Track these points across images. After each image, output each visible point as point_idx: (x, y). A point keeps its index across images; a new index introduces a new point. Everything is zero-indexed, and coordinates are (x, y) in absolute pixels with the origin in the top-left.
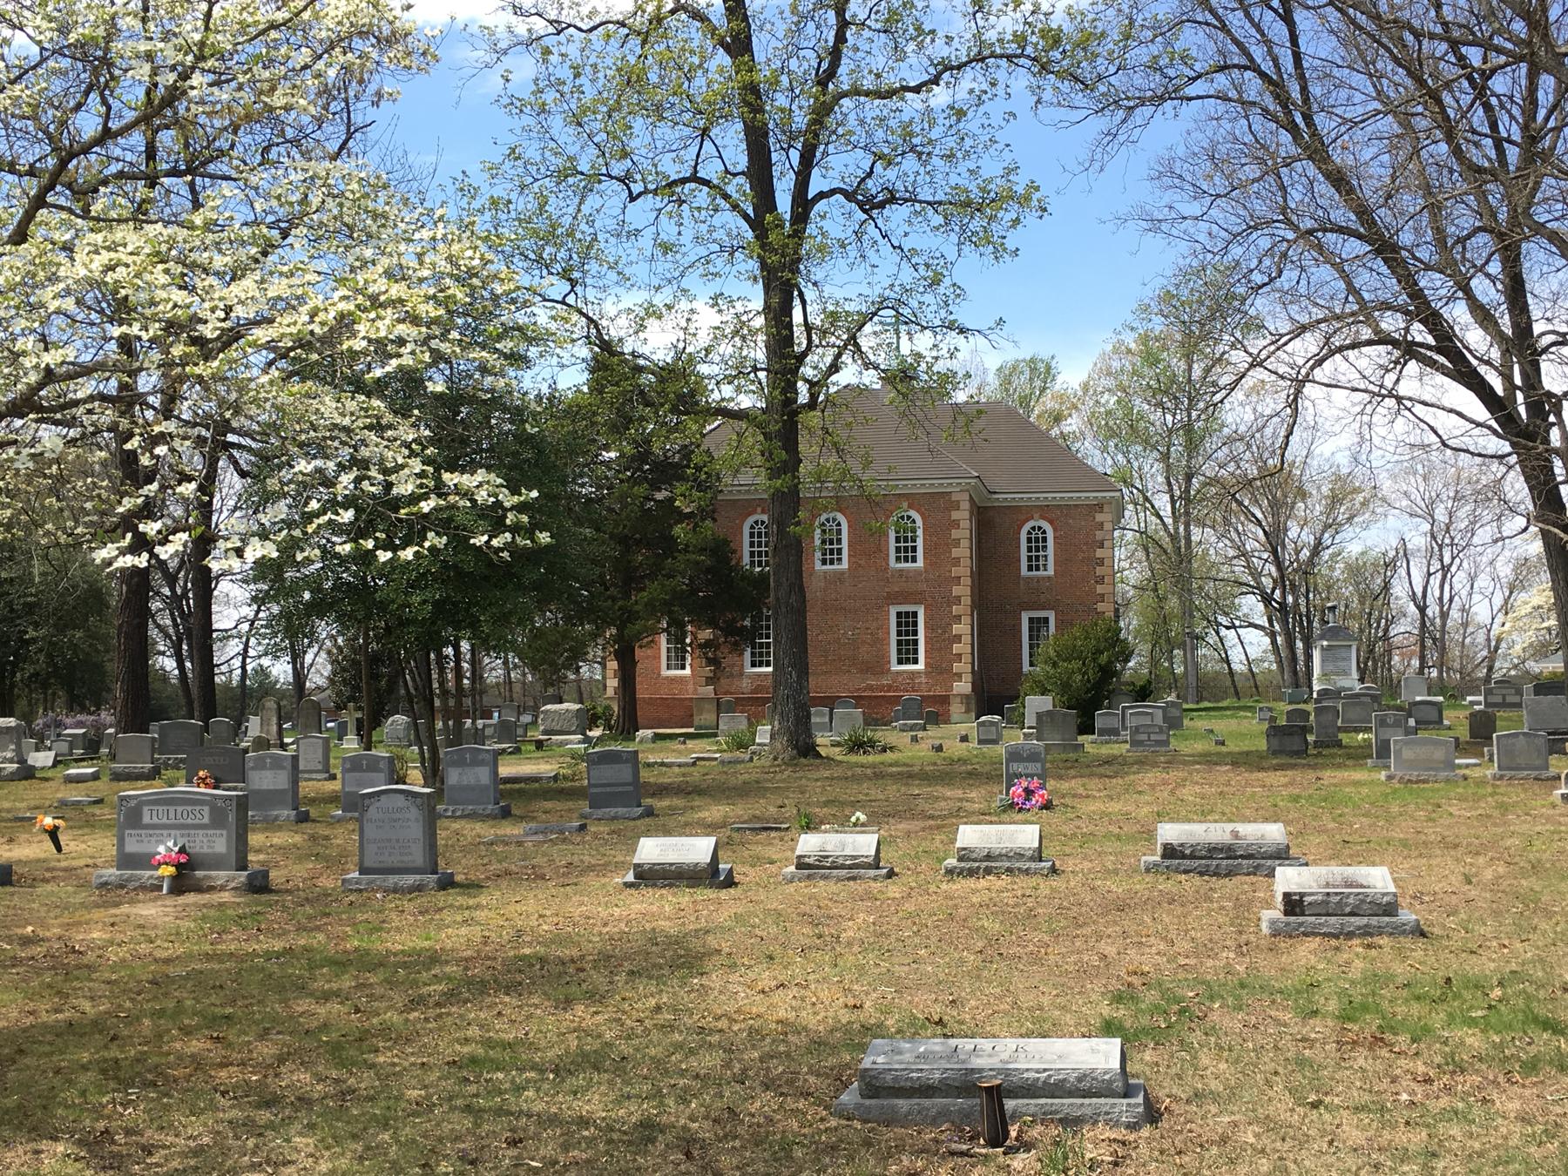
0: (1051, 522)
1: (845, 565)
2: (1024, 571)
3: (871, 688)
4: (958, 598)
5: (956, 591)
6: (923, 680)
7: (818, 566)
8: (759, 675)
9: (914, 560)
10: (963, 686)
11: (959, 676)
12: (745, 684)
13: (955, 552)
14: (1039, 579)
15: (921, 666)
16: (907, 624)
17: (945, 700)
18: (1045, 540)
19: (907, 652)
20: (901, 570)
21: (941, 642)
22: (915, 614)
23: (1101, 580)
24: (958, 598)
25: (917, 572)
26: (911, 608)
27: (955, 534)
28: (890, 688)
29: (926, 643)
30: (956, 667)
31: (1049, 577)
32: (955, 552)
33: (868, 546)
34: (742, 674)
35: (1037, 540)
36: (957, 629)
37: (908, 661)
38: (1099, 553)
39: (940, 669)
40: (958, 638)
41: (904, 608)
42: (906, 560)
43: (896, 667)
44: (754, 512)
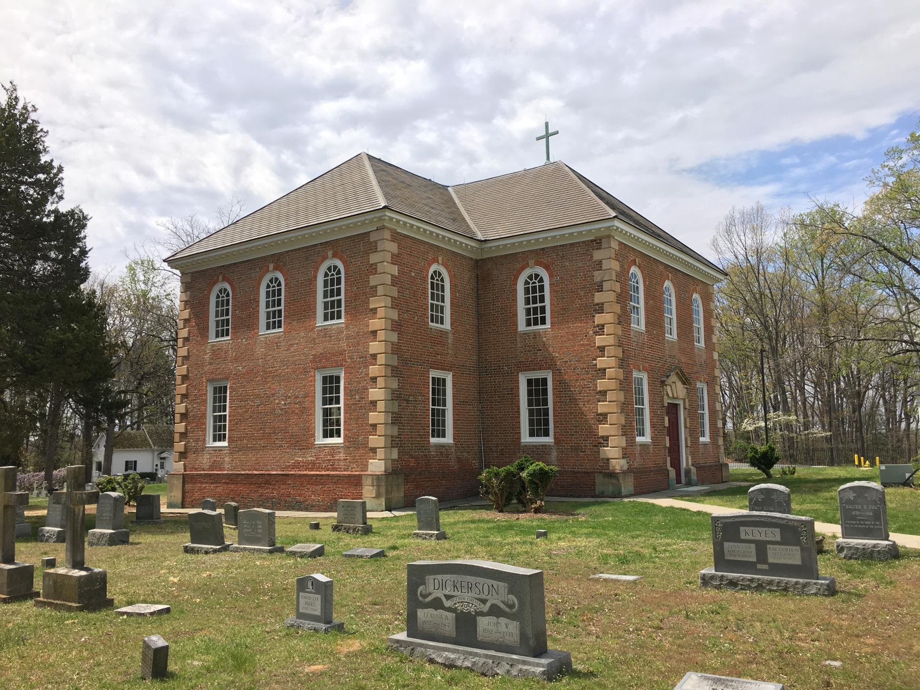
0: (547, 268)
2: (522, 326)
3: (297, 466)
6: (342, 456)
11: (374, 450)
12: (205, 460)
14: (536, 335)
17: (356, 482)
18: (542, 288)
24: (374, 356)
28: (313, 465)
34: (204, 448)
35: (534, 288)
39: (358, 447)
41: (329, 373)
43: (320, 440)
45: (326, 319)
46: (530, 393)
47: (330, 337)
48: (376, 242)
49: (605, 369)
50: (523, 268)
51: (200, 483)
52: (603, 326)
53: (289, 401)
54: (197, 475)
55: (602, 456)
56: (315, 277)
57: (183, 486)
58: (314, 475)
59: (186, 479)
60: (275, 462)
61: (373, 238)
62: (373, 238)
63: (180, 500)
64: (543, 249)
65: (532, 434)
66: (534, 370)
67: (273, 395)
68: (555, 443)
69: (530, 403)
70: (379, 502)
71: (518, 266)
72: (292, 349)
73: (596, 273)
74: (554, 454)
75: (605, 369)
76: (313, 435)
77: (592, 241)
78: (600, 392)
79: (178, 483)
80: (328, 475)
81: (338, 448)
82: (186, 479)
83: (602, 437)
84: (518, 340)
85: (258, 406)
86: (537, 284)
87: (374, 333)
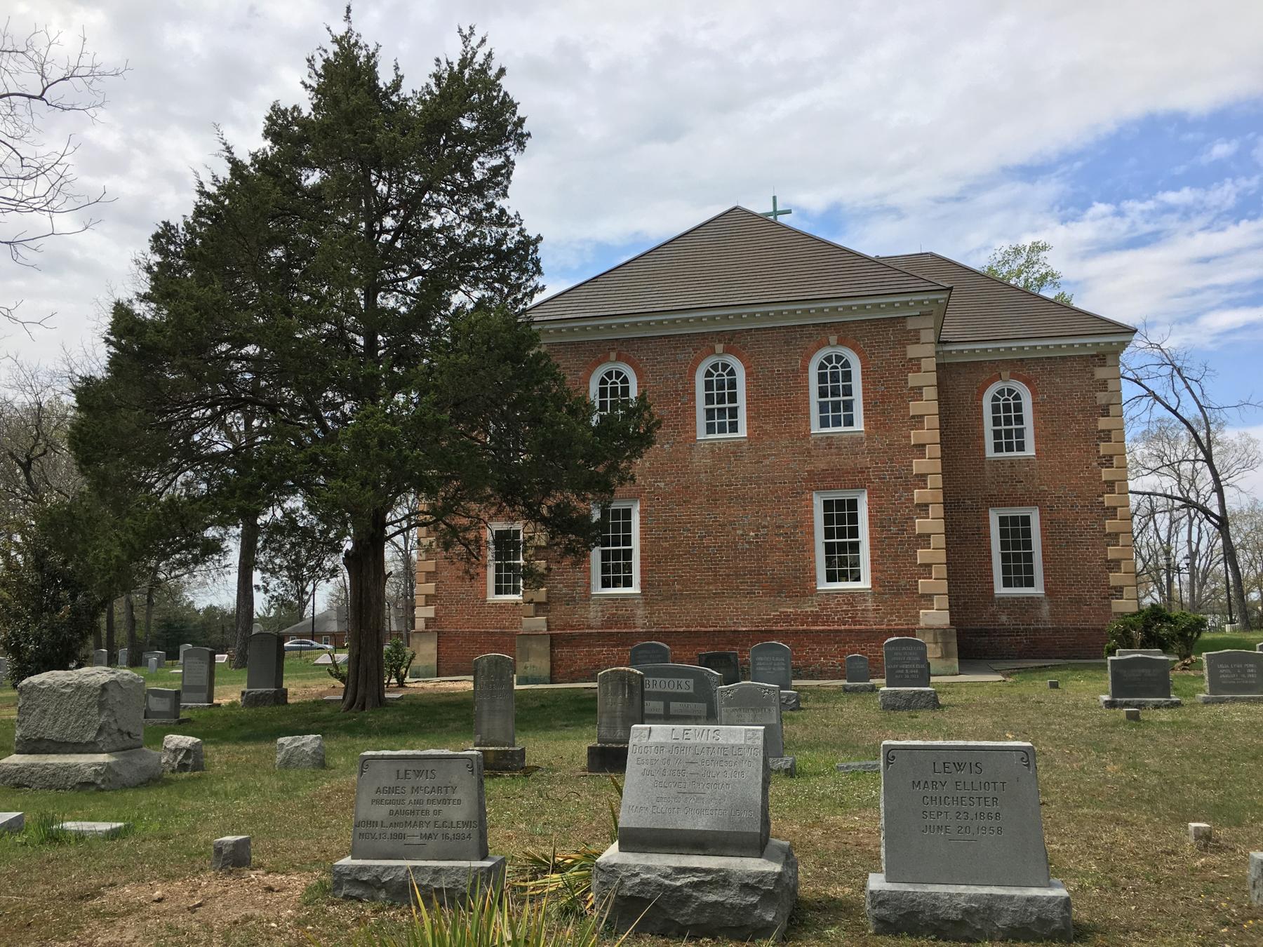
0: (1028, 382)
1: (743, 432)
2: (990, 453)
3: (786, 618)
4: (922, 478)
5: (918, 466)
6: (870, 605)
7: (702, 435)
8: (613, 599)
9: (849, 422)
10: (936, 615)
13: (915, 408)
14: (1012, 463)
15: (865, 583)
16: (841, 520)
19: (841, 565)
20: (829, 438)
21: (896, 543)
22: (853, 504)
23: (1108, 461)
25: (855, 440)
26: (846, 495)
27: (913, 379)
28: (816, 618)
29: (873, 547)
30: (923, 585)
31: (1028, 460)
32: (915, 408)
33: (778, 404)
34: (587, 597)
35: (1007, 408)
36: (921, 525)
37: (843, 576)
38: (1103, 423)
40: (924, 539)
42: (837, 423)
43: (824, 585)
44: (605, 359)
45: (824, 423)
46: (1003, 533)
47: (839, 448)
48: (917, 331)
49: (1115, 508)
50: (992, 381)
51: (589, 646)
52: (1111, 456)
53: (763, 531)
54: (581, 635)
55: (1114, 610)
56: (806, 369)
57: (552, 652)
58: (823, 631)
59: (555, 641)
60: (739, 613)
61: (910, 325)
62: (910, 325)
63: (548, 671)
64: (1022, 360)
65: (1007, 583)
66: (1013, 505)
67: (731, 523)
68: (1046, 594)
69: (1004, 545)
70: (949, 663)
71: (984, 377)
72: (767, 462)
73: (1100, 395)
74: (1046, 608)
75: (1115, 508)
76: (814, 578)
77: (1092, 356)
78: (1110, 534)
79: (544, 647)
80: (851, 631)
81: (862, 594)
82: (555, 641)
83: (1114, 588)
84: (987, 468)
85: (701, 538)
86: (1012, 402)
87: (922, 446)
